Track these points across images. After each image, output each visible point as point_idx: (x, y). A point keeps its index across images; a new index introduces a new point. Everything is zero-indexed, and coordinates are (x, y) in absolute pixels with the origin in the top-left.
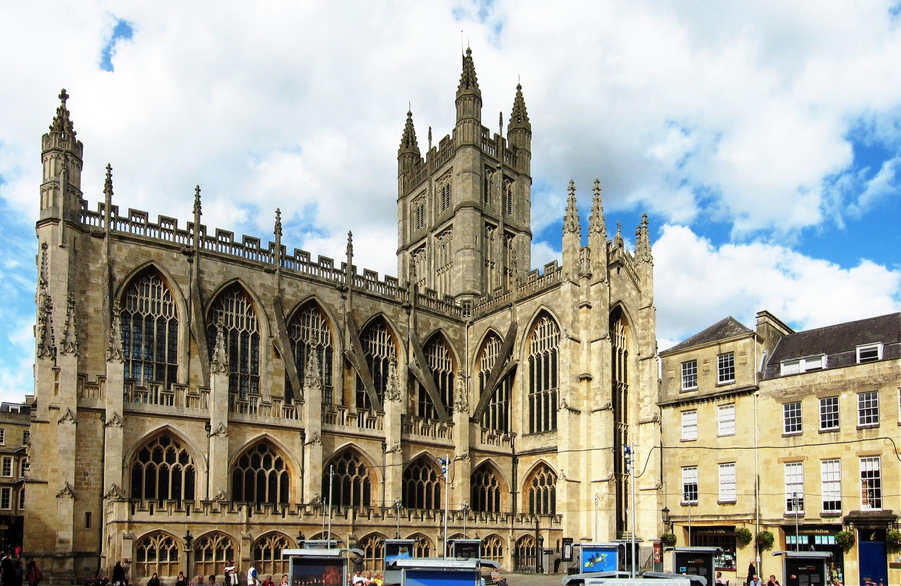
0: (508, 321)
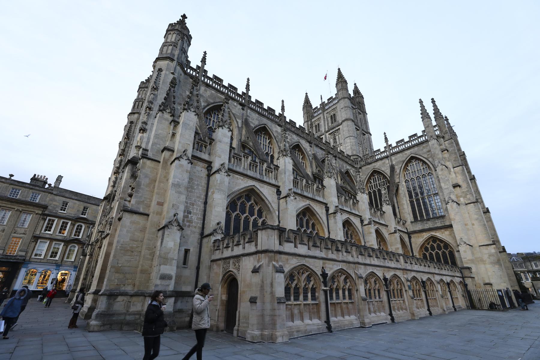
0: (387, 164)
